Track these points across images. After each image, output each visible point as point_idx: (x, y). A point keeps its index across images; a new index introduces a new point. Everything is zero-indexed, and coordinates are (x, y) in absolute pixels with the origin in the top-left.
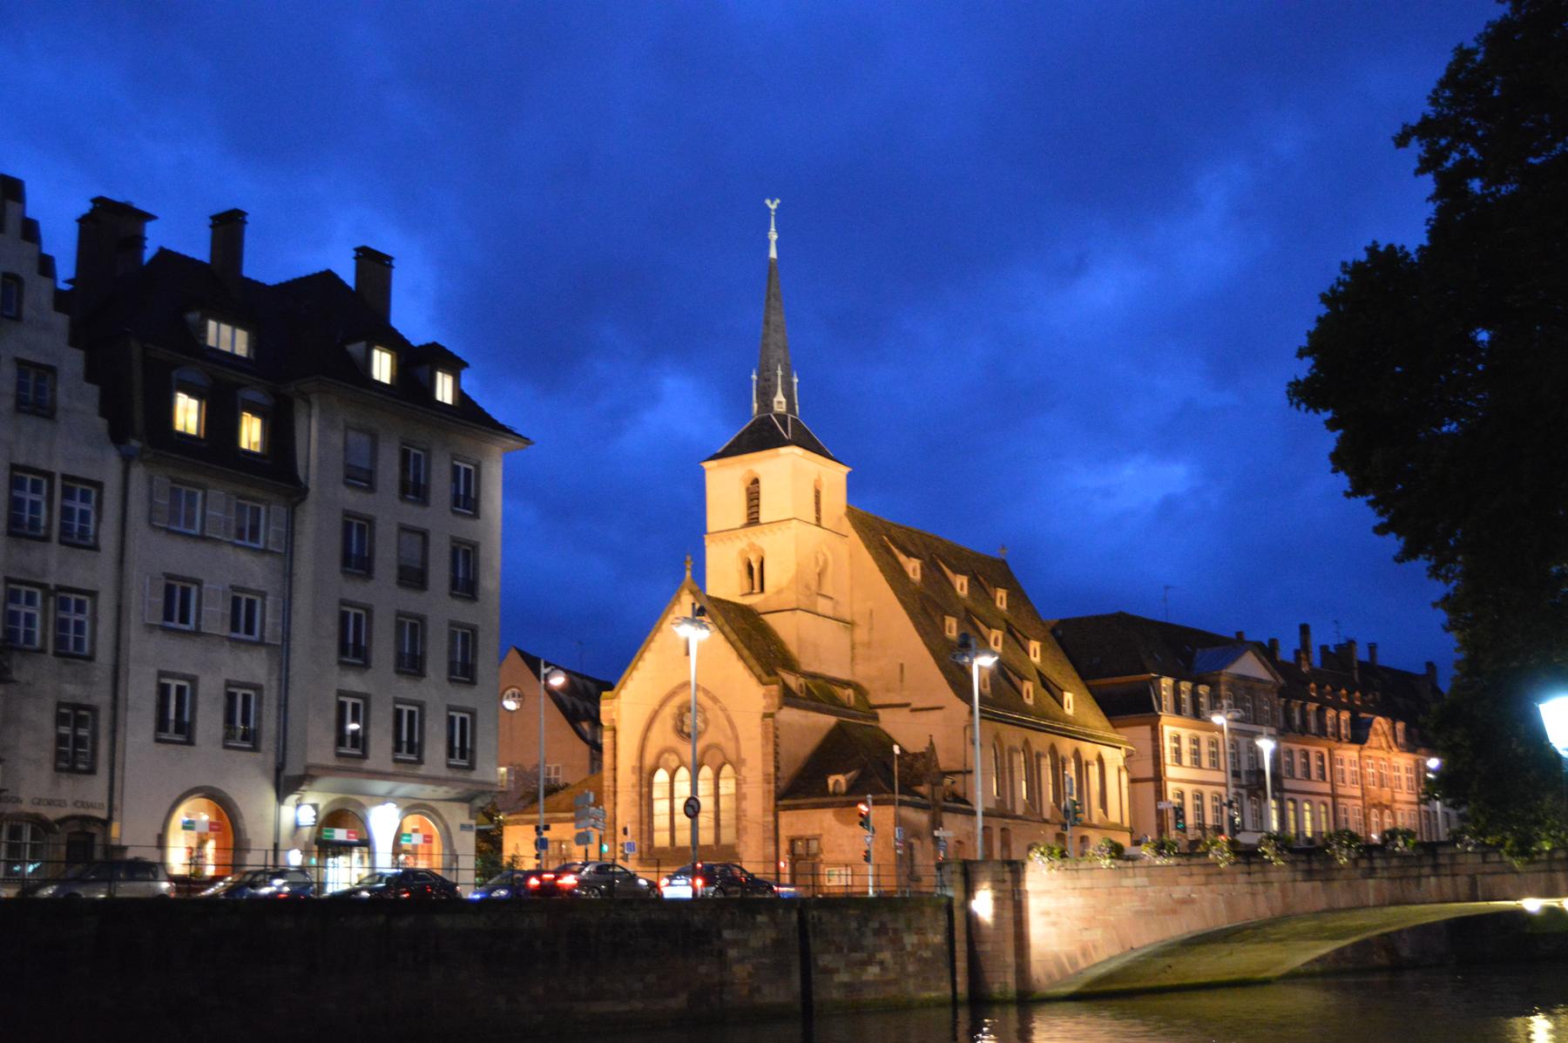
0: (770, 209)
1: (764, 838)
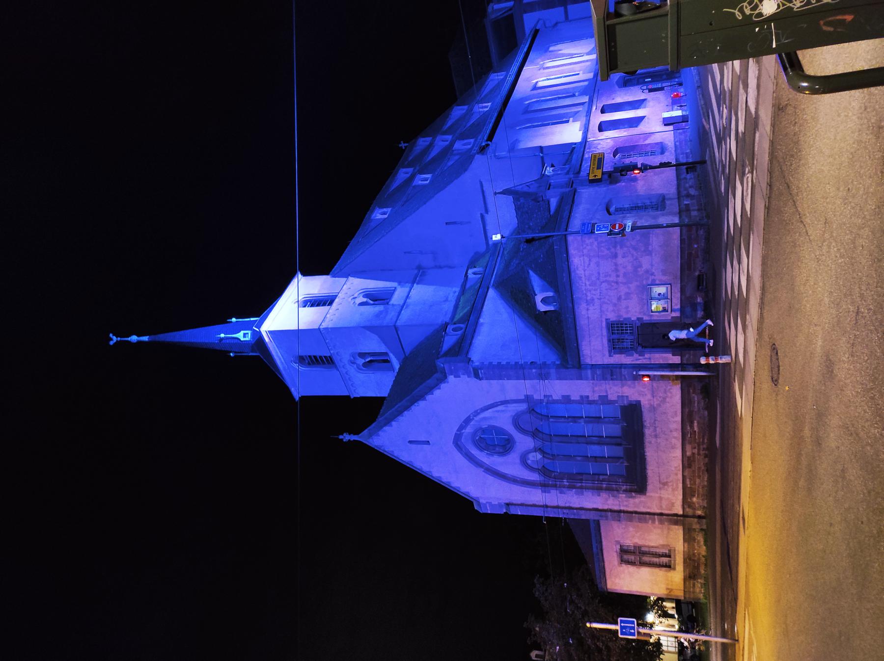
0: (117, 341)
1: (612, 379)
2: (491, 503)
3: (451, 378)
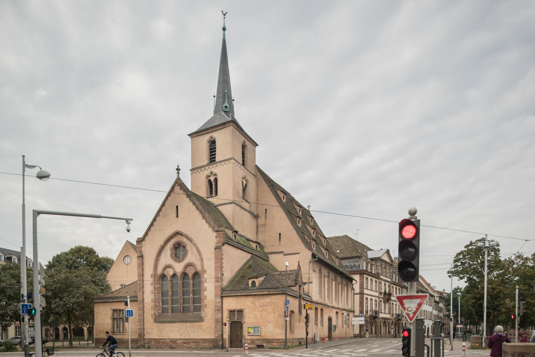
1: (216, 310)
2: (143, 247)
3: (215, 234)
